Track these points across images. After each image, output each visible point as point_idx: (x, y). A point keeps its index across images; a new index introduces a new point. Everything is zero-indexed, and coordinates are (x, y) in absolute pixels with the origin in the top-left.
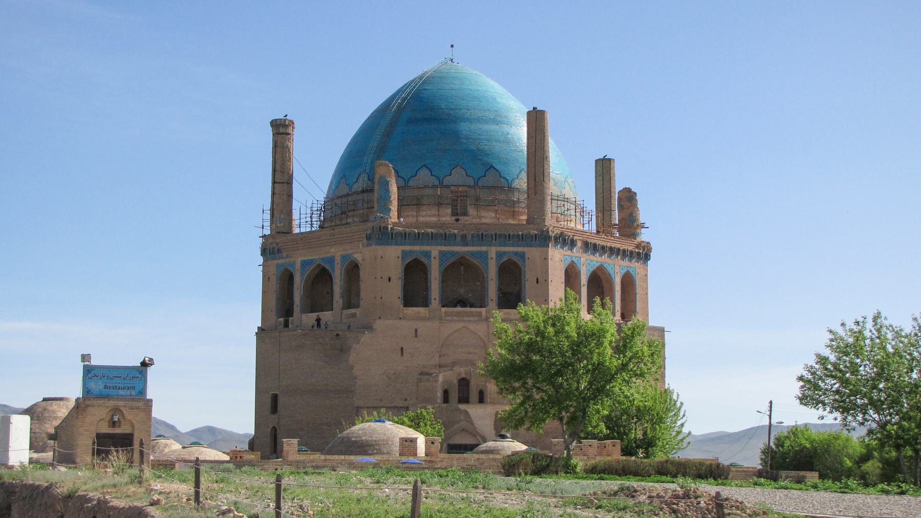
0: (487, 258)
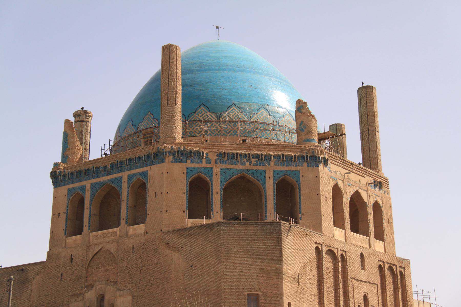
0: (122, 183)
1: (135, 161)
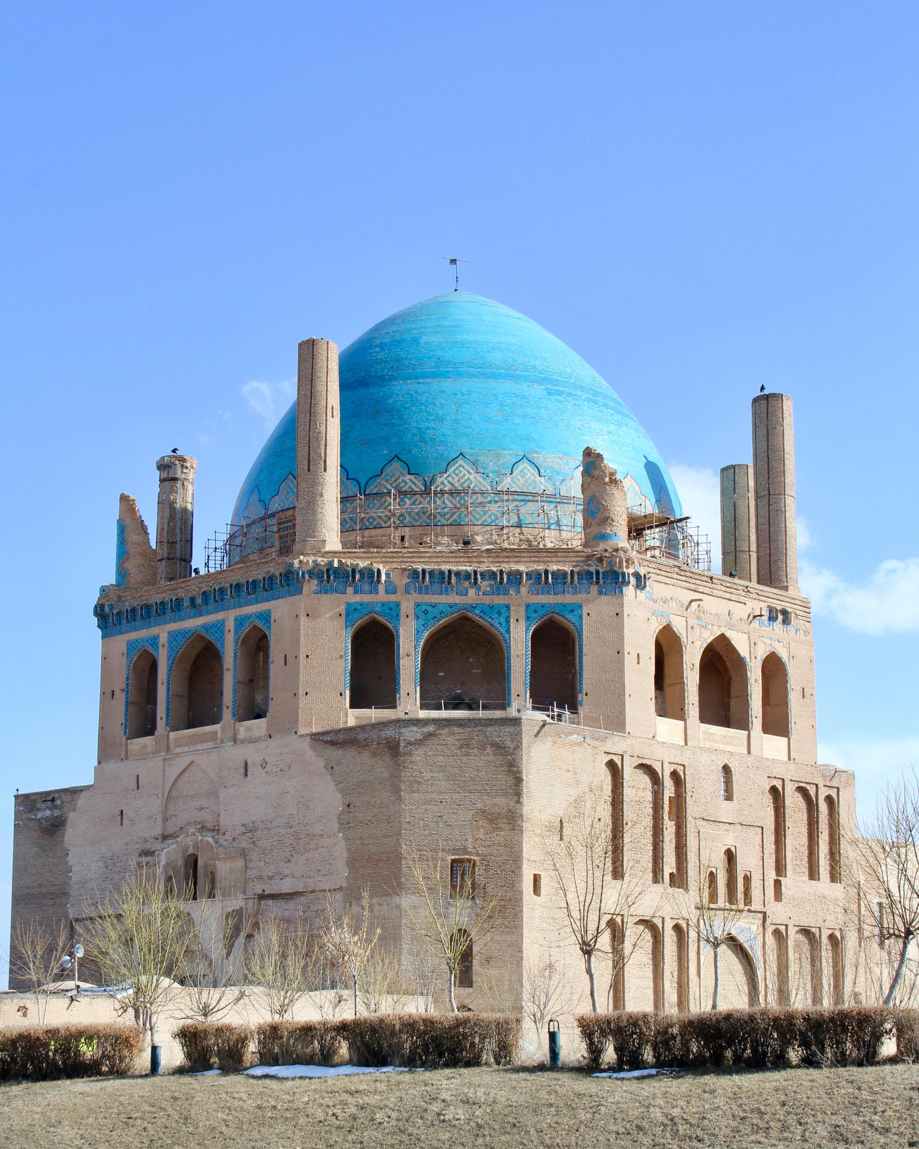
0: (223, 632)
1: (247, 589)
